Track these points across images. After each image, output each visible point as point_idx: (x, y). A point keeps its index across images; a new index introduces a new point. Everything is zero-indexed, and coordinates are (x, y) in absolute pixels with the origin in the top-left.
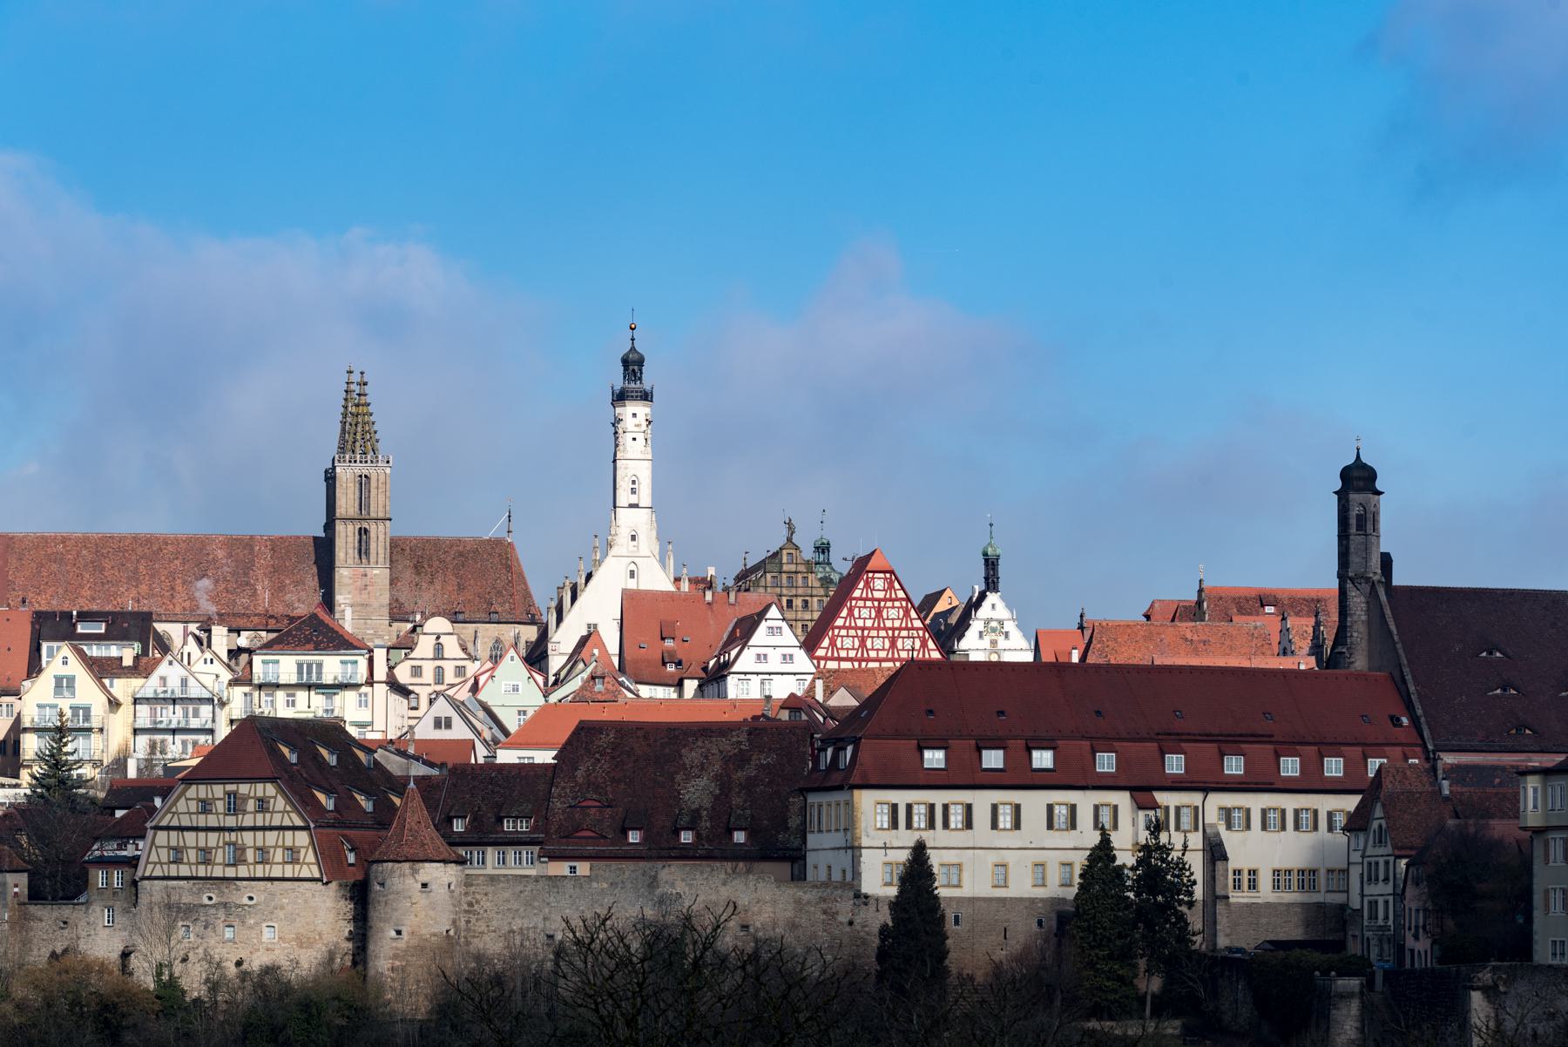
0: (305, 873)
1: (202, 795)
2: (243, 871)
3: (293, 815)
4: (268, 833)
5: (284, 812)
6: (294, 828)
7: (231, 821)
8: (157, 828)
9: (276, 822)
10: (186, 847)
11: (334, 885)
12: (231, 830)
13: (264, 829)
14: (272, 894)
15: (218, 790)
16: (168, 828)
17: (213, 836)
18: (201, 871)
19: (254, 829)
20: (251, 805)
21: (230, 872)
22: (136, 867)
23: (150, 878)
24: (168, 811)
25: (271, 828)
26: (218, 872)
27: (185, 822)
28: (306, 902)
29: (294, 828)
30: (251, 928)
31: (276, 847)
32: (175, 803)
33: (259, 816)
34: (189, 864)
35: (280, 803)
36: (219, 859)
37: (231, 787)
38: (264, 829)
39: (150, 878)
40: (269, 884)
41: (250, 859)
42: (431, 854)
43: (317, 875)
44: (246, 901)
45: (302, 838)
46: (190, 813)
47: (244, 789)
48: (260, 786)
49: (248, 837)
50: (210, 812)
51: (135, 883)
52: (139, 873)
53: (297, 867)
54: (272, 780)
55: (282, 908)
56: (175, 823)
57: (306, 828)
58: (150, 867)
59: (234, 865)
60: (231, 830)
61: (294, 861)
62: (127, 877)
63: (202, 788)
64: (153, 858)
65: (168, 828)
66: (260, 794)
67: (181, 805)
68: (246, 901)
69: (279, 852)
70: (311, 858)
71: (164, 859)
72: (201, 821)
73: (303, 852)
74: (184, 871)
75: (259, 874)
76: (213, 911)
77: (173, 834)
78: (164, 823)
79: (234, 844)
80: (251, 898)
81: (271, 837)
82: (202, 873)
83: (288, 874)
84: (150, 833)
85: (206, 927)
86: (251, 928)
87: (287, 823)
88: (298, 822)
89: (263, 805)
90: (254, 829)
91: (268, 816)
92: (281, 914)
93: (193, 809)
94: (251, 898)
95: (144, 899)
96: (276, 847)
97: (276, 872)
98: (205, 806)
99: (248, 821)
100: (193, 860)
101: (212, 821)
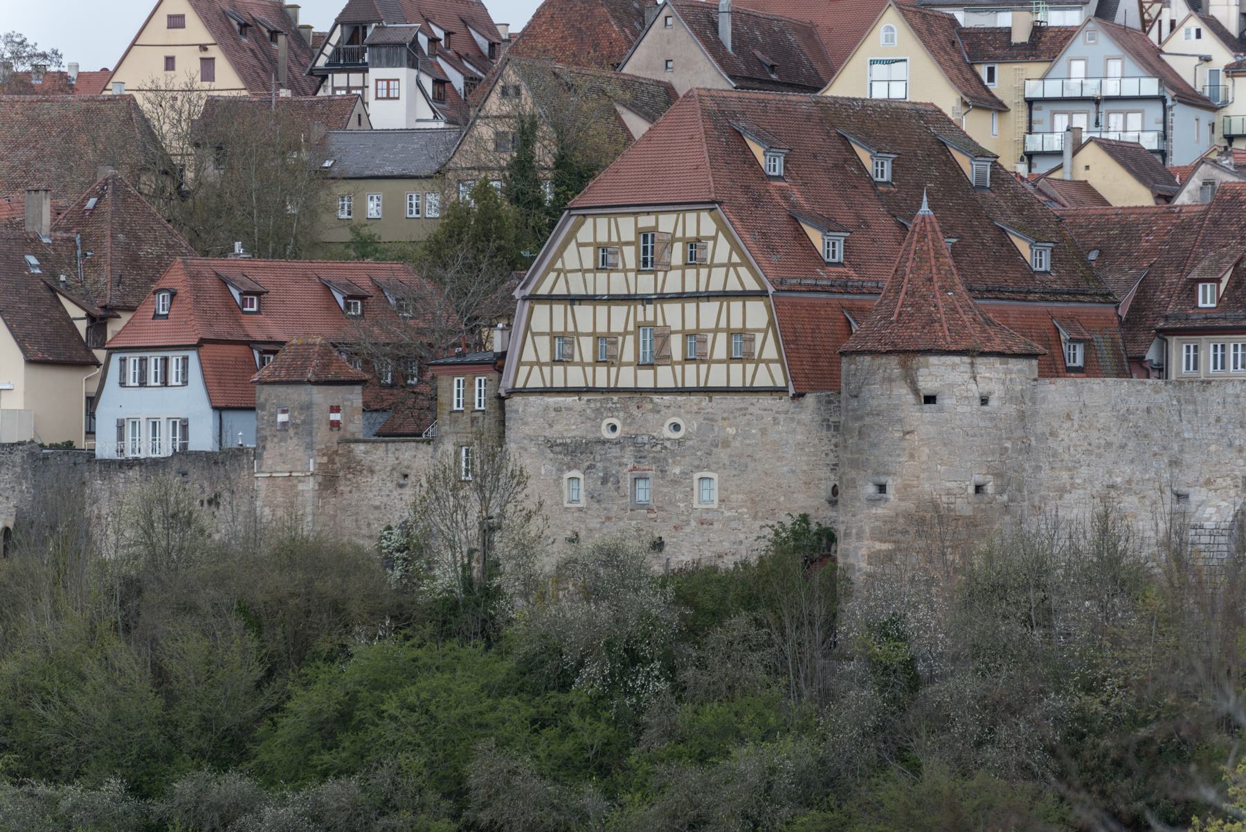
0: (762, 380)
1: (602, 238)
2: (665, 377)
3: (743, 271)
4: (704, 305)
5: (729, 265)
6: (744, 295)
7: (646, 284)
8: (535, 298)
9: (716, 286)
10: (577, 334)
11: (810, 399)
12: (645, 300)
13: (697, 297)
14: (711, 419)
15: (627, 228)
16: (551, 299)
17: (619, 311)
18: (601, 378)
19: (681, 297)
20: (677, 255)
21: (646, 379)
22: (500, 370)
23: (525, 391)
24: (551, 268)
25: (709, 296)
26: (626, 378)
27: (577, 289)
28: (764, 432)
29: (744, 295)
30: (675, 482)
31: (716, 330)
32: (560, 254)
33: (691, 273)
34: (583, 364)
35: (723, 250)
36: (628, 356)
37: (646, 221)
38: (697, 297)
39: (525, 391)
40: (704, 401)
41: (677, 355)
42: (947, 342)
43: (781, 383)
44: (667, 432)
45: (757, 314)
46: (585, 271)
47: (666, 223)
48: (691, 218)
49: (672, 312)
50: (614, 268)
51: (501, 399)
52: (507, 384)
53: (750, 367)
54: (710, 205)
55: (726, 444)
56: (560, 289)
57: (761, 294)
58: (524, 370)
59: (651, 366)
60: (645, 300)
61: (747, 358)
62: (492, 393)
63: (602, 222)
64: (528, 355)
65: (551, 299)
66: (691, 233)
67: (570, 258)
68: (667, 432)
69: (722, 338)
70: (771, 351)
71: (545, 357)
72: (601, 284)
73: (759, 337)
74: (576, 377)
75: (691, 382)
76: (615, 451)
77: (559, 309)
78: (544, 290)
79: (653, 324)
80: (676, 427)
81: (709, 310)
82: (601, 383)
83: (736, 382)
84: (522, 309)
85: (604, 481)
86: (675, 482)
87: (733, 285)
88: (752, 285)
89: (694, 253)
90: (681, 297)
91: (704, 272)
92: (722, 454)
93: (589, 263)
94: (676, 427)
95: (516, 432)
96: (716, 330)
97: (717, 377)
98: (605, 258)
99: (673, 284)
100: (588, 357)
101: (618, 283)
